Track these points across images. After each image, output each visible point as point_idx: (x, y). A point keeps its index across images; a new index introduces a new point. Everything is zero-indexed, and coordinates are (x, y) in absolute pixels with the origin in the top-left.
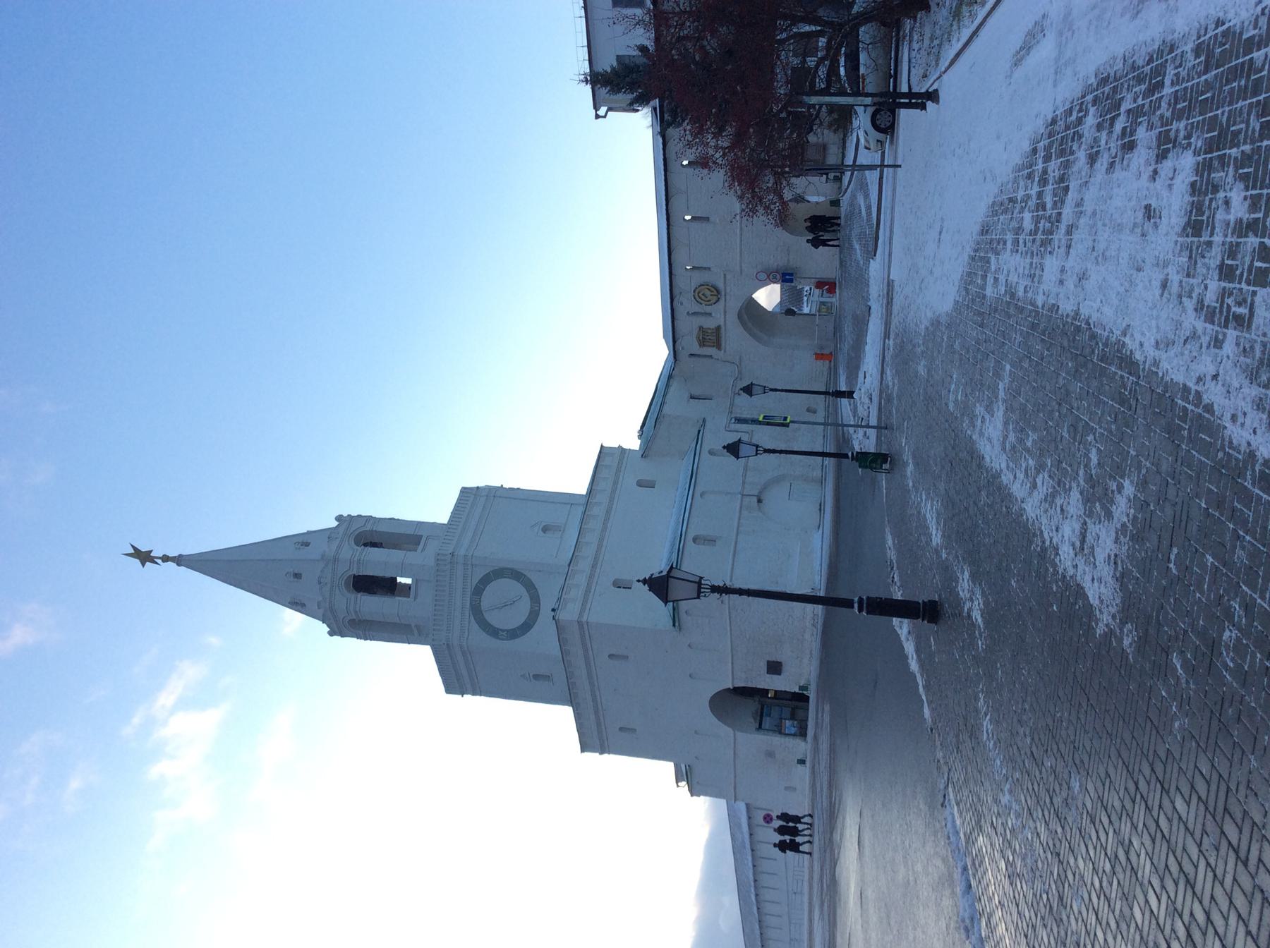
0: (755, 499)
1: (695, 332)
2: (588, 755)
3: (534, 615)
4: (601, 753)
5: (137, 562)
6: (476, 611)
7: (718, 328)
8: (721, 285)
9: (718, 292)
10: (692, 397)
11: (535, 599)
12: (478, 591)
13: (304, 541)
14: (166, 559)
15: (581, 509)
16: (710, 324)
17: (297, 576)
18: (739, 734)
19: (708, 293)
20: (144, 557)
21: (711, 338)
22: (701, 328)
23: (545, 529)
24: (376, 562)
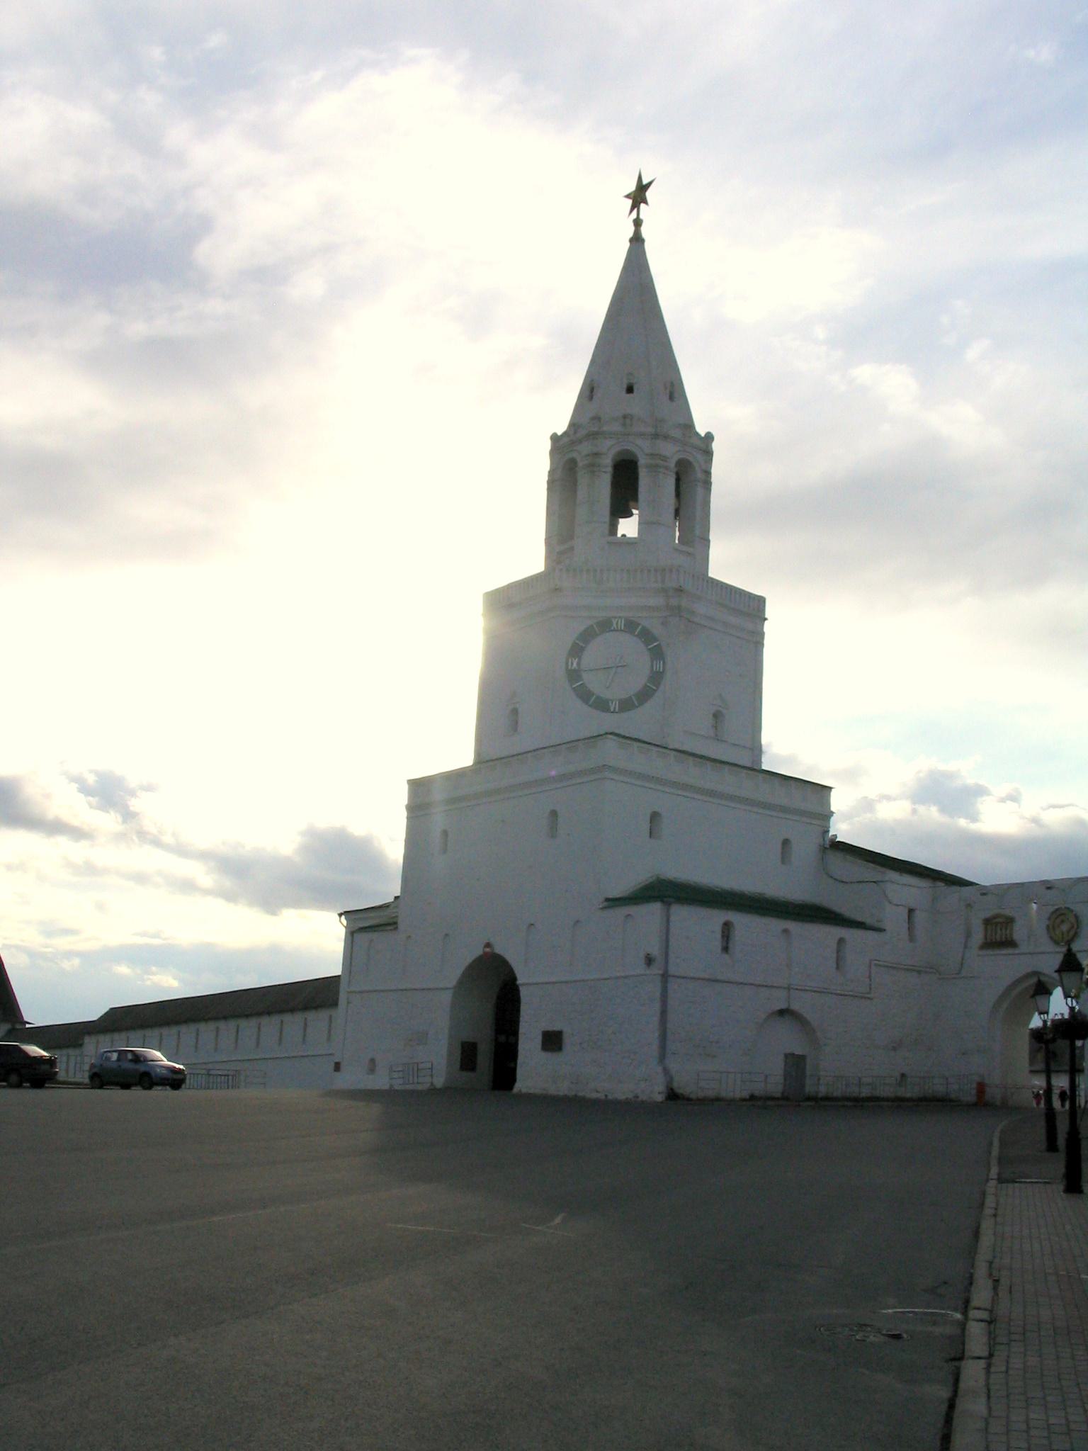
0: (784, 1006)
1: (1008, 912)
2: (405, 788)
3: (602, 705)
5: (632, 187)
7: (1010, 943)
10: (911, 911)
11: (627, 705)
13: (674, 391)
14: (638, 223)
15: (749, 765)
17: (630, 390)
18: (447, 997)
19: (1065, 927)
20: (639, 196)
22: (1010, 921)
23: (717, 716)
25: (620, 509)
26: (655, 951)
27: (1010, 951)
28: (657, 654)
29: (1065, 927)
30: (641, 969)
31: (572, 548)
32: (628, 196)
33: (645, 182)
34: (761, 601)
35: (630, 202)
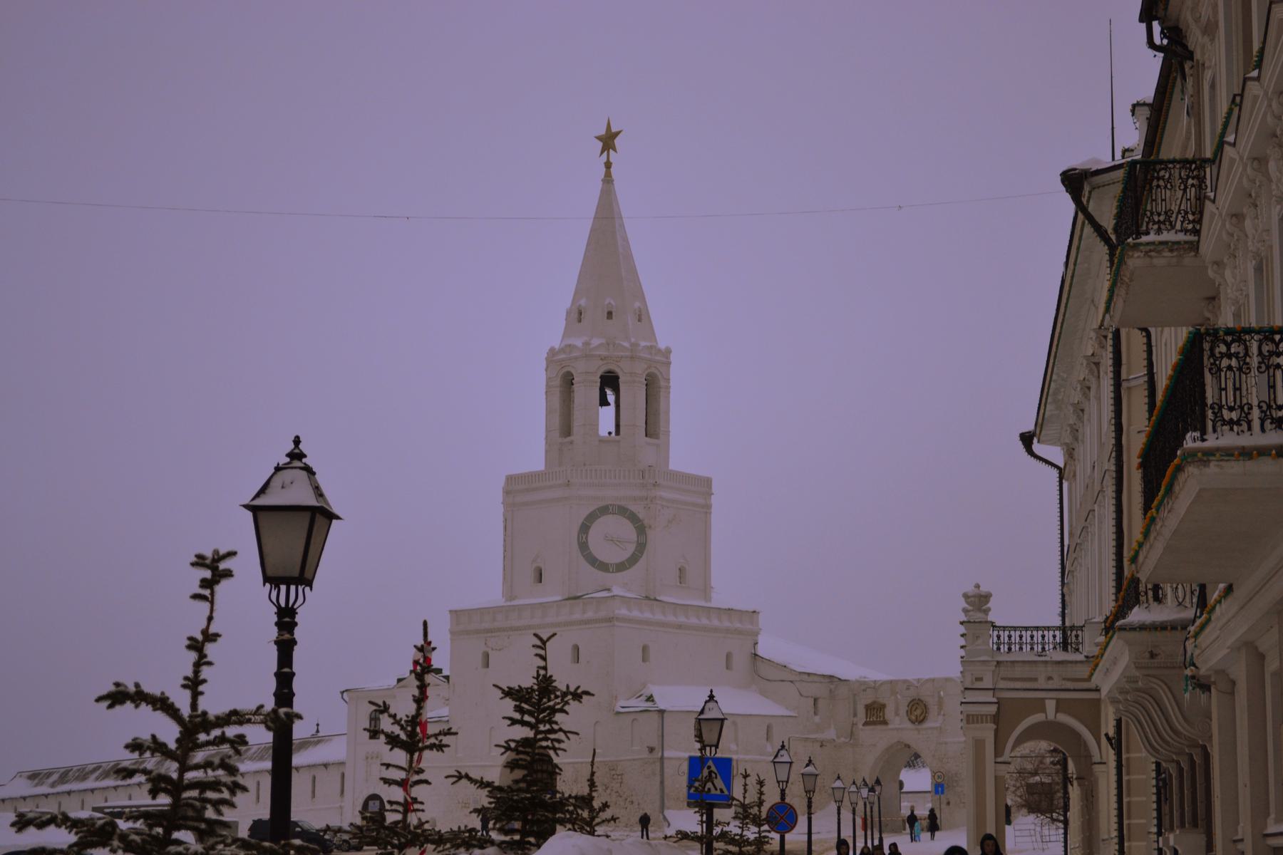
4: (452, 633)
5: (602, 131)
6: (604, 510)
7: (885, 723)
8: (926, 725)
9: (921, 722)
10: (815, 700)
12: (623, 511)
14: (608, 165)
16: (889, 713)
19: (918, 712)
21: (875, 714)
22: (883, 707)
23: (681, 570)
24: (633, 394)
25: (604, 402)
26: (655, 744)
27: (883, 727)
28: (641, 529)
29: (918, 712)
30: (646, 755)
31: (571, 443)
32: (599, 138)
33: (614, 130)
34: (708, 482)
35: (600, 144)
